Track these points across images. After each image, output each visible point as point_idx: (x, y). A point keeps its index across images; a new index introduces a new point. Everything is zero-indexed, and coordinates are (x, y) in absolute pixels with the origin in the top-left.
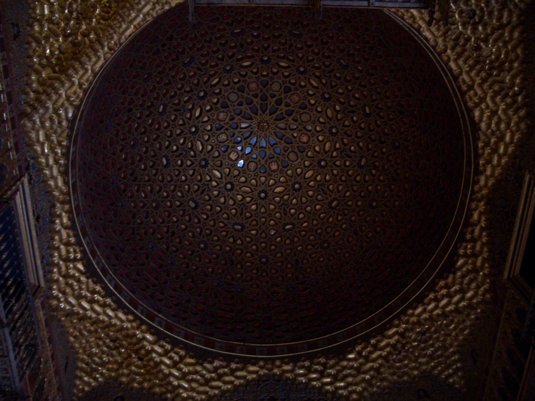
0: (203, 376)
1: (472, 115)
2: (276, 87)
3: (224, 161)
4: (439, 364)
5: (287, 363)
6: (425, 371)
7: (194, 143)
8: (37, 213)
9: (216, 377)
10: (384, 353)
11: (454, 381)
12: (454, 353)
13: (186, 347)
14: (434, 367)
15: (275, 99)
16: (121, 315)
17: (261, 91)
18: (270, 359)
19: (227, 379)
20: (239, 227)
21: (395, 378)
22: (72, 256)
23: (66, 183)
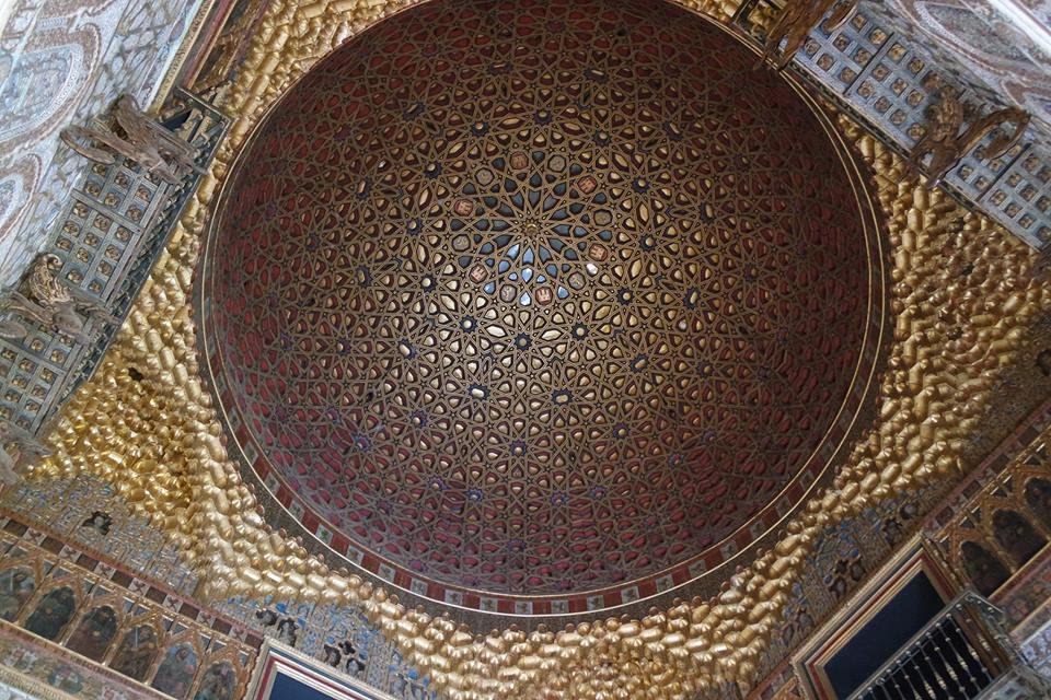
0: (733, 615)
2: (484, 177)
3: (541, 313)
5: (823, 495)
6: (1030, 314)
8: (341, 645)
9: (751, 600)
13: (684, 596)
17: (478, 199)
18: (799, 508)
19: (766, 589)
20: (642, 361)
22: (440, 636)
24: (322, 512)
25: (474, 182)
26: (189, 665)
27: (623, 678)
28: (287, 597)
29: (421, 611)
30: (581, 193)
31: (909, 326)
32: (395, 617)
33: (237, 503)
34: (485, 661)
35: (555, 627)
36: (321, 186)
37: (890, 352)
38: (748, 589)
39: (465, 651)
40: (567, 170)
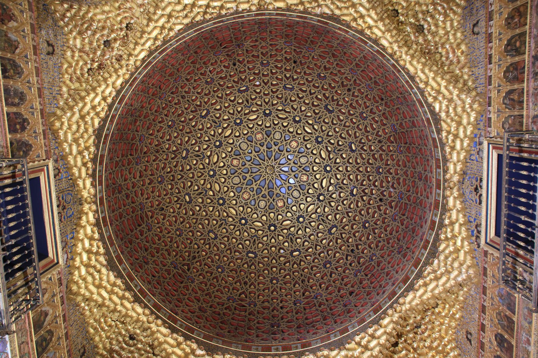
1: (115, 273)
2: (262, 204)
3: (302, 140)
4: (84, 16)
5: (243, 10)
7: (327, 158)
10: (146, 36)
11: (62, 5)
12: (71, 32)
13: (349, 26)
14: (87, 12)
15: (262, 193)
16: (412, 70)
21: (128, 5)
23: (445, 197)
24: (429, 216)
25: (267, 207)
26: (504, 292)
27: (420, 16)
28: (468, 229)
29: (445, 151)
30: (241, 161)
31: (140, 53)
32: (455, 164)
33: (432, 276)
34: (447, 107)
35: (412, 78)
36: (302, 275)
37: (156, 47)
38: (316, 4)
39: (449, 121)
40: (236, 174)
